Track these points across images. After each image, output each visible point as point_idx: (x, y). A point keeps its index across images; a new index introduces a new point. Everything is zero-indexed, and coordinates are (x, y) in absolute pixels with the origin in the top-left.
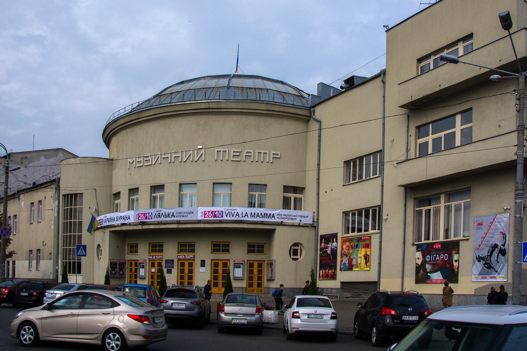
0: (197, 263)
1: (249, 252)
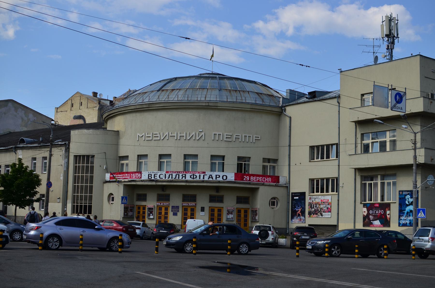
0: (198, 208)
1: (238, 202)
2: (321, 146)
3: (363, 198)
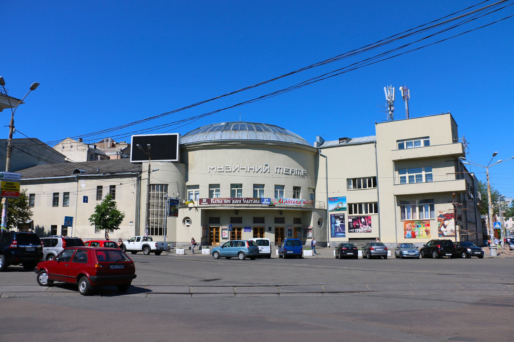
2: (368, 178)
3: (403, 217)
